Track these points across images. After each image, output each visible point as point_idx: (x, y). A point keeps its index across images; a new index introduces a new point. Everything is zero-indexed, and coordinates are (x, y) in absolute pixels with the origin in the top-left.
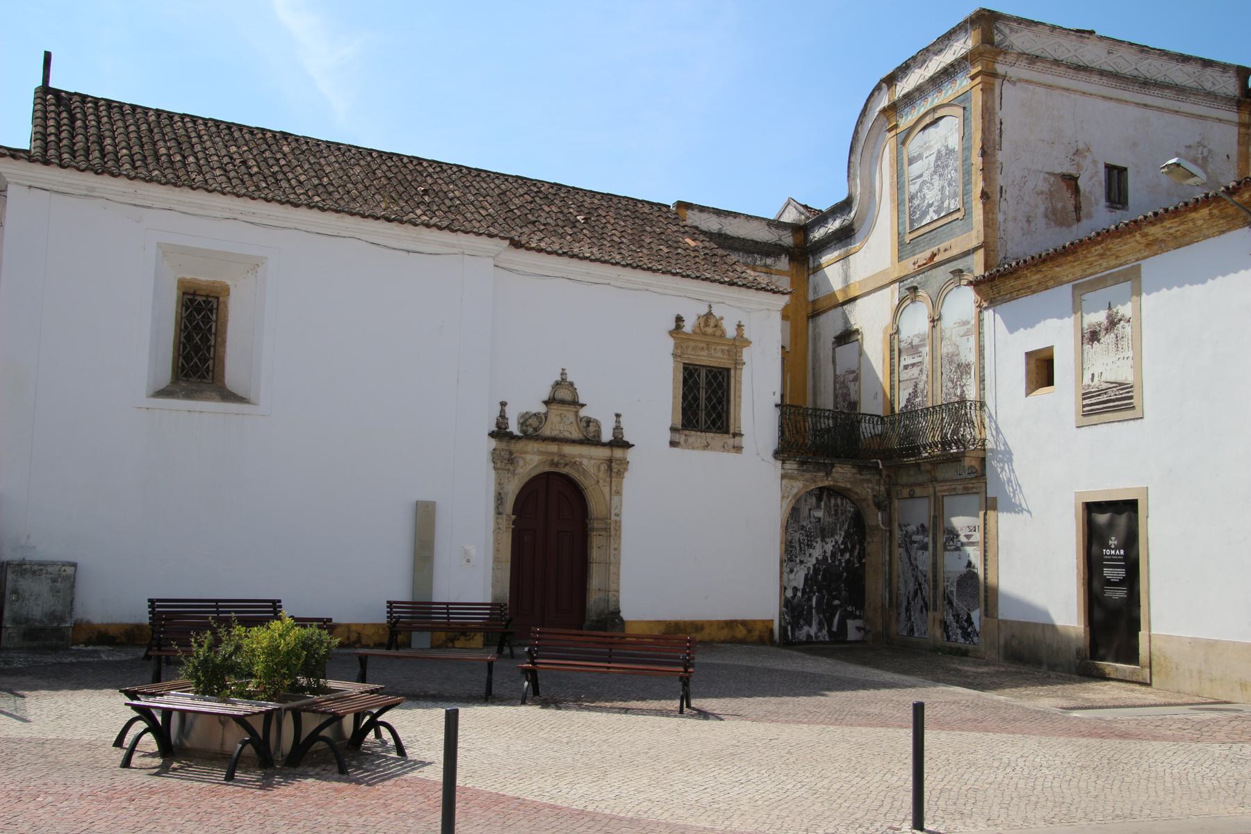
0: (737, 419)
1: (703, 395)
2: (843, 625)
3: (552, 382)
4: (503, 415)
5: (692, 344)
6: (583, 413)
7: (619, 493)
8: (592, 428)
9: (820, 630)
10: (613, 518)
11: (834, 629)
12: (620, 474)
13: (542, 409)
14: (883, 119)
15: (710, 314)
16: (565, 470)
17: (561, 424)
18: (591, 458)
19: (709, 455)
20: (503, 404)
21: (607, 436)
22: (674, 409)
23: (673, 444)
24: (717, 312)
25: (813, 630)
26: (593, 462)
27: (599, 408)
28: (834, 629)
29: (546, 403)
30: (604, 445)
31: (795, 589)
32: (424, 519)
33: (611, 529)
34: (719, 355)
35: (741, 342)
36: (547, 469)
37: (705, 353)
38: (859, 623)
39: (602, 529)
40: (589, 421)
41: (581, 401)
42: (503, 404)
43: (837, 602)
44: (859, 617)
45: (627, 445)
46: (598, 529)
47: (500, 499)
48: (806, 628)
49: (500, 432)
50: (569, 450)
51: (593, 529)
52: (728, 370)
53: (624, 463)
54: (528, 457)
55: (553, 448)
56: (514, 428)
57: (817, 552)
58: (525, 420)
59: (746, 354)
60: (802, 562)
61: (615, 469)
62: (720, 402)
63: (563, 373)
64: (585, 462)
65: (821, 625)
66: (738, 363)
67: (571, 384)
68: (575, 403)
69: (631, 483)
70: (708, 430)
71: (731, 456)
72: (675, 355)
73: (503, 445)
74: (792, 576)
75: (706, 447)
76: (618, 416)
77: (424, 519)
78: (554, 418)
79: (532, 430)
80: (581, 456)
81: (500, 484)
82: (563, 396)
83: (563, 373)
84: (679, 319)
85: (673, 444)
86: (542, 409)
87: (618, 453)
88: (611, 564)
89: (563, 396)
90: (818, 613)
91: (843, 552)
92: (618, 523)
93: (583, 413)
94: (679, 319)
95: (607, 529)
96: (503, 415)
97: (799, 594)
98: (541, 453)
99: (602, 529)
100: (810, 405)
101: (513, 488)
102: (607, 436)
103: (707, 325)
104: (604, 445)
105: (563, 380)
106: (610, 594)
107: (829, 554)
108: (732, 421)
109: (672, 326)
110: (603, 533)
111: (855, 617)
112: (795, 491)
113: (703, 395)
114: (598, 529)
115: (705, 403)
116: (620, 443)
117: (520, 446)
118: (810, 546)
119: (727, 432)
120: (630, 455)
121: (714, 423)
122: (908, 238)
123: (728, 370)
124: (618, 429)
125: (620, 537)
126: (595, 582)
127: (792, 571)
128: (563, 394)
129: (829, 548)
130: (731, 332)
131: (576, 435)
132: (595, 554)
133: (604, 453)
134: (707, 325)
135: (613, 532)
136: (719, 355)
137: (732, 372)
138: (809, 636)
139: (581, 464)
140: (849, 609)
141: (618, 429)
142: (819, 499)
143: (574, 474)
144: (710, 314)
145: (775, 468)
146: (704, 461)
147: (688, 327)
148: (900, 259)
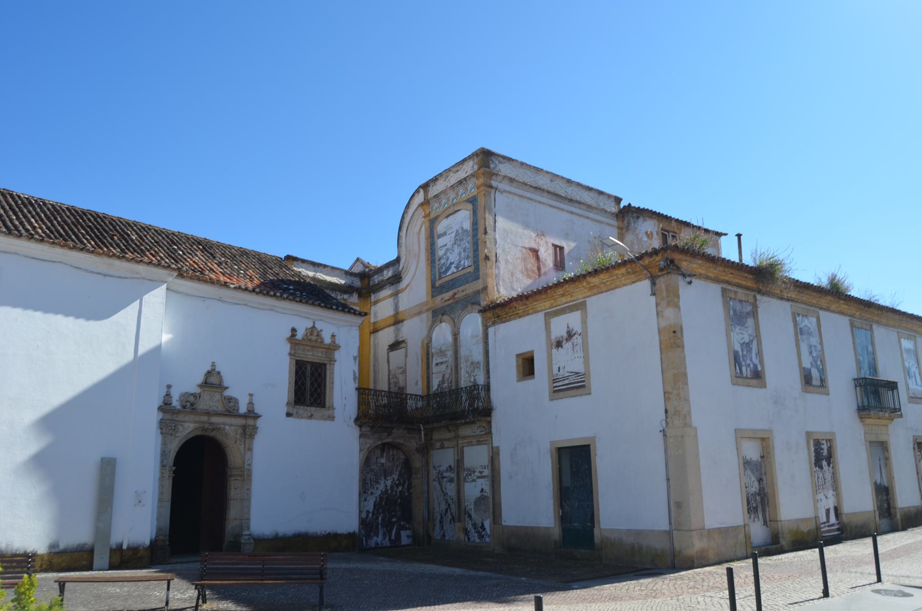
0: (332, 397)
1: (308, 382)
2: (398, 535)
3: (205, 371)
4: (168, 395)
5: (302, 347)
6: (227, 393)
7: (250, 449)
8: (231, 404)
9: (384, 539)
10: (246, 467)
11: (393, 537)
12: (252, 436)
14: (420, 211)
15: (314, 327)
16: (212, 434)
18: (231, 425)
19: (313, 423)
21: (243, 409)
22: (289, 391)
23: (289, 415)
24: (319, 326)
25: (379, 539)
26: (233, 428)
27: (238, 389)
28: (393, 537)
29: (201, 386)
30: (241, 416)
31: (368, 512)
32: (108, 469)
33: (246, 475)
34: (320, 354)
35: (334, 347)
36: (199, 433)
37: (310, 353)
38: (409, 532)
39: (238, 475)
40: (230, 399)
41: (226, 384)
42: (169, 387)
43: (394, 520)
44: (409, 529)
45: (257, 417)
47: (164, 454)
48: (375, 538)
49: (166, 407)
50: (215, 419)
51: (231, 476)
52: (325, 365)
53: (255, 428)
54: (186, 425)
55: (205, 418)
56: (176, 403)
57: (381, 487)
58: (185, 396)
59: (337, 355)
60: (372, 493)
61: (248, 432)
62: (319, 385)
63: (213, 364)
64: (227, 428)
65: (384, 534)
66: (332, 360)
67: (219, 373)
68: (221, 387)
69: (259, 443)
70: (311, 405)
71: (328, 423)
72: (290, 354)
73: (168, 416)
74: (366, 503)
75: (311, 417)
76: (251, 395)
77: (108, 469)
78: (206, 396)
79: (190, 404)
80: (224, 424)
81: (164, 444)
82: (212, 381)
83: (213, 364)
84: (294, 330)
85: (289, 415)
86: (198, 390)
87: (250, 422)
88: (246, 500)
89: (212, 381)
90: (383, 527)
91: (398, 486)
92: (249, 471)
93: (227, 393)
94: (294, 330)
95: (242, 476)
96: (168, 395)
97: (370, 515)
98: (195, 422)
99: (238, 475)
100: (371, 387)
101: (174, 446)
102: (243, 409)
103: (311, 334)
104: (241, 416)
105: (214, 370)
106: (245, 521)
107: (389, 487)
108: (327, 399)
109: (289, 334)
111: (406, 529)
112: (368, 445)
113: (308, 382)
115: (309, 386)
116: (252, 415)
117: (180, 417)
118: (377, 482)
119: (324, 406)
120: (260, 423)
121: (315, 400)
122: (437, 284)
123: (325, 365)
124: (251, 403)
126: (233, 512)
127: (365, 500)
128: (213, 380)
129: (389, 483)
130: (327, 340)
131: (220, 409)
132: (233, 493)
134: (311, 334)
135: (246, 477)
136: (320, 354)
137: (328, 367)
138: (377, 543)
140: (402, 523)
141: (251, 403)
142: (383, 451)
143: (219, 437)
144: (314, 327)
145: (355, 431)
146: (308, 427)
147: (299, 336)
148: (433, 297)
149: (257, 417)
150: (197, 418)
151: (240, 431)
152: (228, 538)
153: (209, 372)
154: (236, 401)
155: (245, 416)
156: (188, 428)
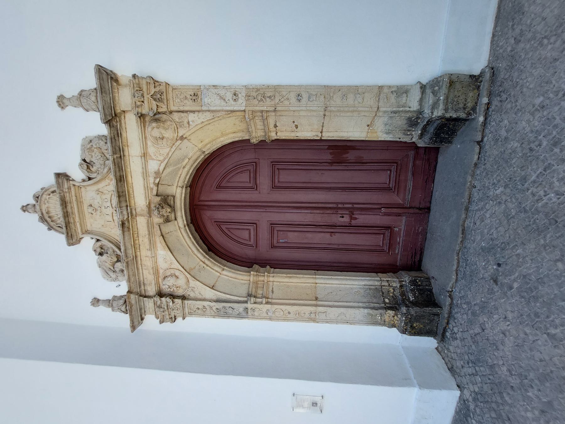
4: (109, 303)
10: (241, 104)
13: (88, 243)
17: (99, 208)
18: (145, 155)
20: (96, 302)
26: (151, 150)
29: (72, 239)
42: (96, 302)
46: (266, 131)
50: (140, 199)
55: (141, 223)
56: (122, 289)
61: (158, 103)
63: (25, 209)
64: (153, 166)
79: (118, 256)
80: (145, 174)
82: (60, 209)
83: (25, 209)
86: (88, 243)
87: (124, 99)
88: (328, 96)
89: (60, 209)
96: (109, 303)
98: (152, 245)
110: (271, 122)
114: (266, 131)
117: (147, 276)
125: (276, 88)
133: (131, 127)
135: (267, 105)
139: (158, 174)
143: (185, 174)
149: (106, 78)
150: (143, 240)
151: (154, 131)
152: (414, 137)
153: (42, 219)
154: (89, 144)
155: (112, 118)
156: (171, 255)
